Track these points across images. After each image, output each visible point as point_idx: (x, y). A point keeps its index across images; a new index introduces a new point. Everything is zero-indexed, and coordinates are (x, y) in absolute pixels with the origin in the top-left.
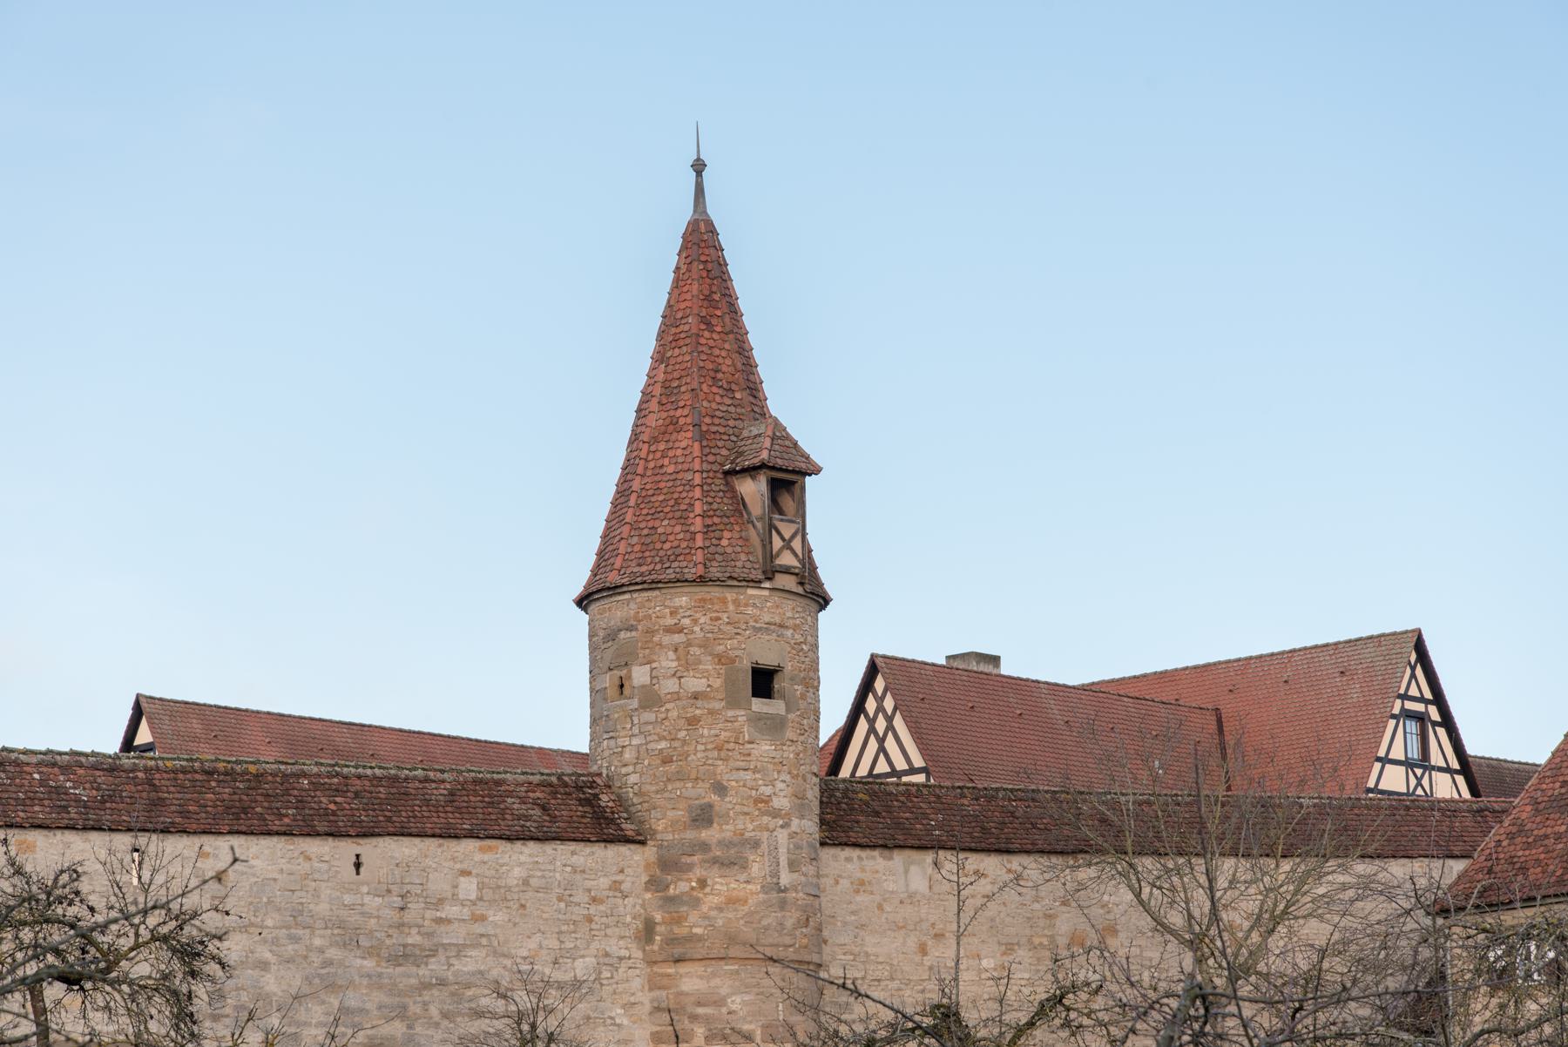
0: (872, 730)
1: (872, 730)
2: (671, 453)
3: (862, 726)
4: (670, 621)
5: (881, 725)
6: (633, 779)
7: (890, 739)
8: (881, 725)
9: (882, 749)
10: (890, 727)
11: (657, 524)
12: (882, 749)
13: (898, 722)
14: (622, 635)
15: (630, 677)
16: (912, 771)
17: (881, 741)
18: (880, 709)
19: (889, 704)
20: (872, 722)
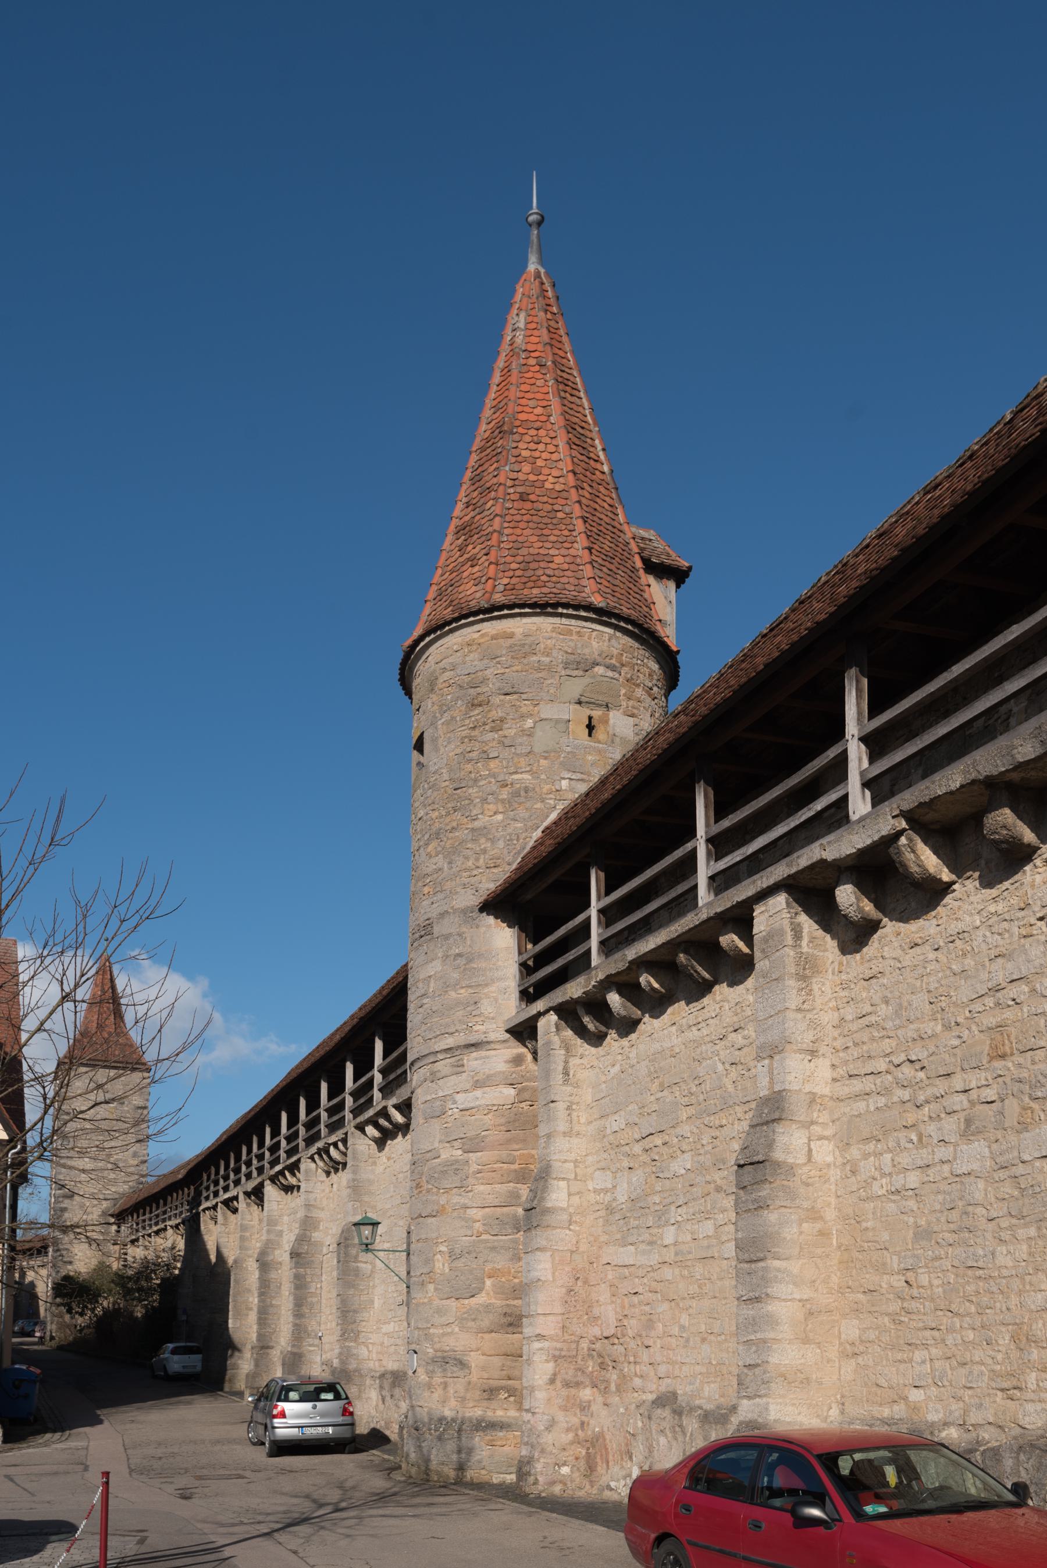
14: (600, 670)
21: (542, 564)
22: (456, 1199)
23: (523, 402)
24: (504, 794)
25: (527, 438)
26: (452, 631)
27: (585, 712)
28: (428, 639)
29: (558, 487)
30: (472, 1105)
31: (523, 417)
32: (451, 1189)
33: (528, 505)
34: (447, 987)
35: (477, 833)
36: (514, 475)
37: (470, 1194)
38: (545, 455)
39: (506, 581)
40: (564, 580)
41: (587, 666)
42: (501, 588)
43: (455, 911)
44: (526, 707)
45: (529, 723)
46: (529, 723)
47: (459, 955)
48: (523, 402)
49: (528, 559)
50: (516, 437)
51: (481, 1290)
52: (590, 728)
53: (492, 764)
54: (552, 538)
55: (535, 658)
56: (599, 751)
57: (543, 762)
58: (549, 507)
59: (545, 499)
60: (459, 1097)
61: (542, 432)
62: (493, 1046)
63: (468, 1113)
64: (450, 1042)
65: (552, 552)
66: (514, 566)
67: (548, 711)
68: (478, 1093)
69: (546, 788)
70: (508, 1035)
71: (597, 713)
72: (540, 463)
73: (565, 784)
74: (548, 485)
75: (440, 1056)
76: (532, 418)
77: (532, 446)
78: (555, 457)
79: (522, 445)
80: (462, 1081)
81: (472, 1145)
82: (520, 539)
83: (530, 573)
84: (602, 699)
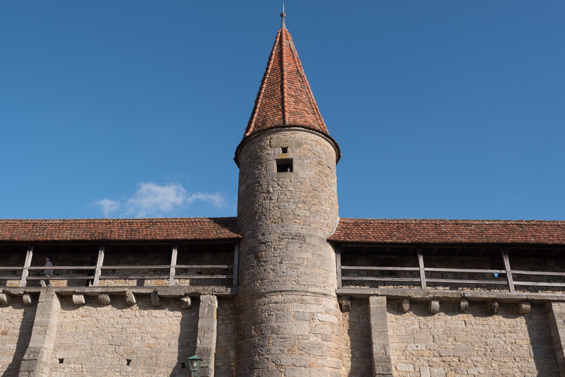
22: (319, 361)
26: (311, 133)
28: (300, 128)
30: (325, 320)
32: (317, 356)
34: (314, 266)
37: (326, 360)
43: (317, 237)
60: (319, 315)
62: (331, 297)
63: (323, 323)
64: (317, 290)
68: (327, 315)
70: (336, 295)
75: (308, 294)
80: (320, 308)
81: (326, 339)
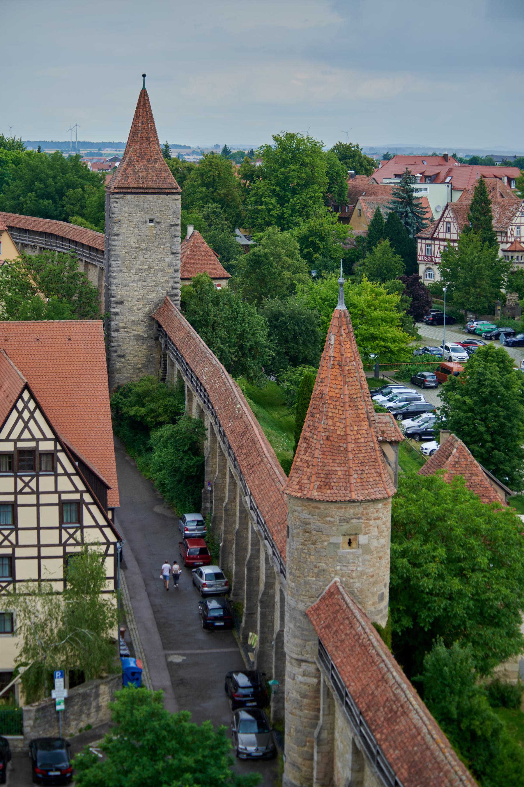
0: (20, 417)
1: (20, 417)
2: (361, 432)
3: (15, 414)
4: (376, 515)
5: (26, 415)
6: (357, 585)
7: (32, 422)
8: (26, 415)
9: (26, 426)
10: (32, 416)
11: (364, 468)
12: (26, 426)
13: (38, 415)
14: (354, 521)
15: (356, 539)
16: (45, 439)
17: (26, 423)
18: (26, 407)
19: (32, 405)
20: (20, 413)
21: (333, 476)
23: (331, 385)
24: (316, 570)
25: (332, 406)
27: (347, 538)
29: (342, 434)
31: (331, 394)
33: (329, 443)
35: (306, 583)
36: (325, 426)
38: (338, 416)
39: (318, 483)
40: (341, 484)
41: (347, 521)
42: (316, 487)
44: (324, 538)
45: (326, 543)
46: (326, 543)
47: (299, 627)
48: (331, 385)
49: (328, 472)
50: (327, 405)
51: (305, 746)
52: (350, 543)
53: (312, 557)
54: (338, 461)
55: (328, 519)
56: (352, 553)
57: (331, 560)
58: (337, 445)
59: (336, 440)
61: (338, 403)
65: (338, 469)
66: (322, 476)
67: (333, 540)
69: (331, 570)
71: (352, 537)
72: (336, 419)
73: (338, 568)
74: (338, 432)
76: (334, 395)
77: (334, 411)
78: (342, 417)
79: (329, 410)
82: (326, 461)
83: (327, 481)
84: (354, 532)
